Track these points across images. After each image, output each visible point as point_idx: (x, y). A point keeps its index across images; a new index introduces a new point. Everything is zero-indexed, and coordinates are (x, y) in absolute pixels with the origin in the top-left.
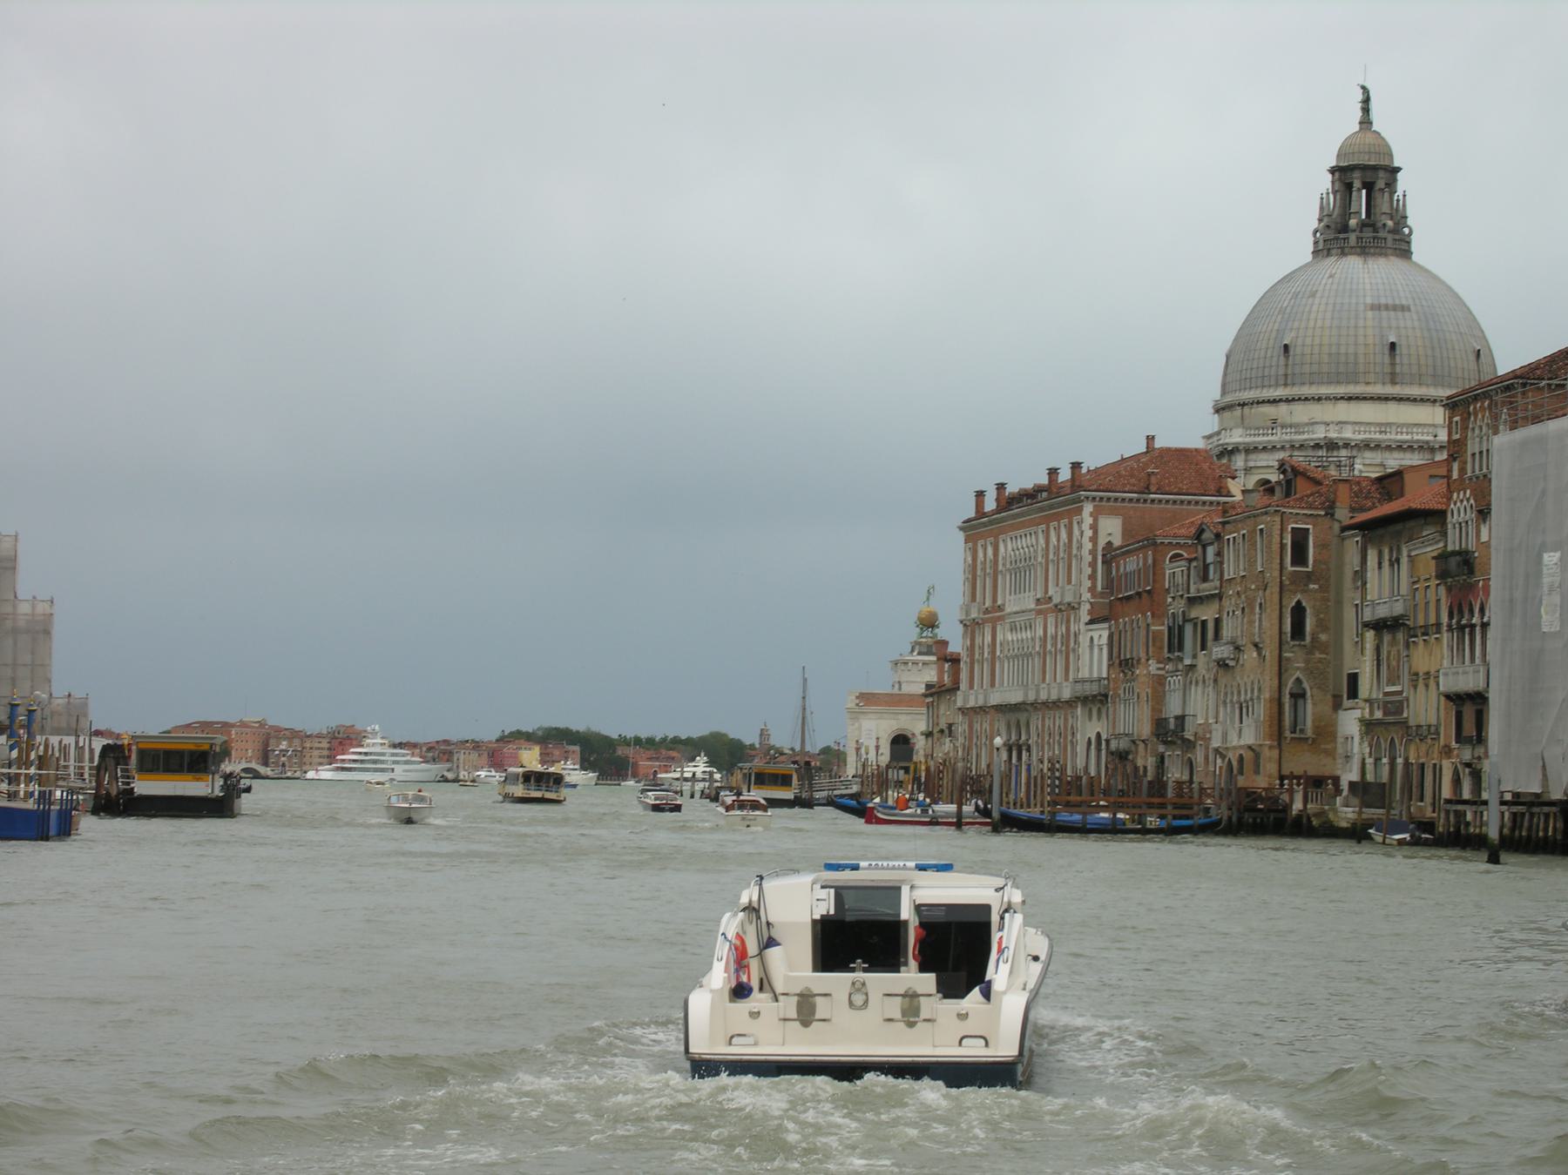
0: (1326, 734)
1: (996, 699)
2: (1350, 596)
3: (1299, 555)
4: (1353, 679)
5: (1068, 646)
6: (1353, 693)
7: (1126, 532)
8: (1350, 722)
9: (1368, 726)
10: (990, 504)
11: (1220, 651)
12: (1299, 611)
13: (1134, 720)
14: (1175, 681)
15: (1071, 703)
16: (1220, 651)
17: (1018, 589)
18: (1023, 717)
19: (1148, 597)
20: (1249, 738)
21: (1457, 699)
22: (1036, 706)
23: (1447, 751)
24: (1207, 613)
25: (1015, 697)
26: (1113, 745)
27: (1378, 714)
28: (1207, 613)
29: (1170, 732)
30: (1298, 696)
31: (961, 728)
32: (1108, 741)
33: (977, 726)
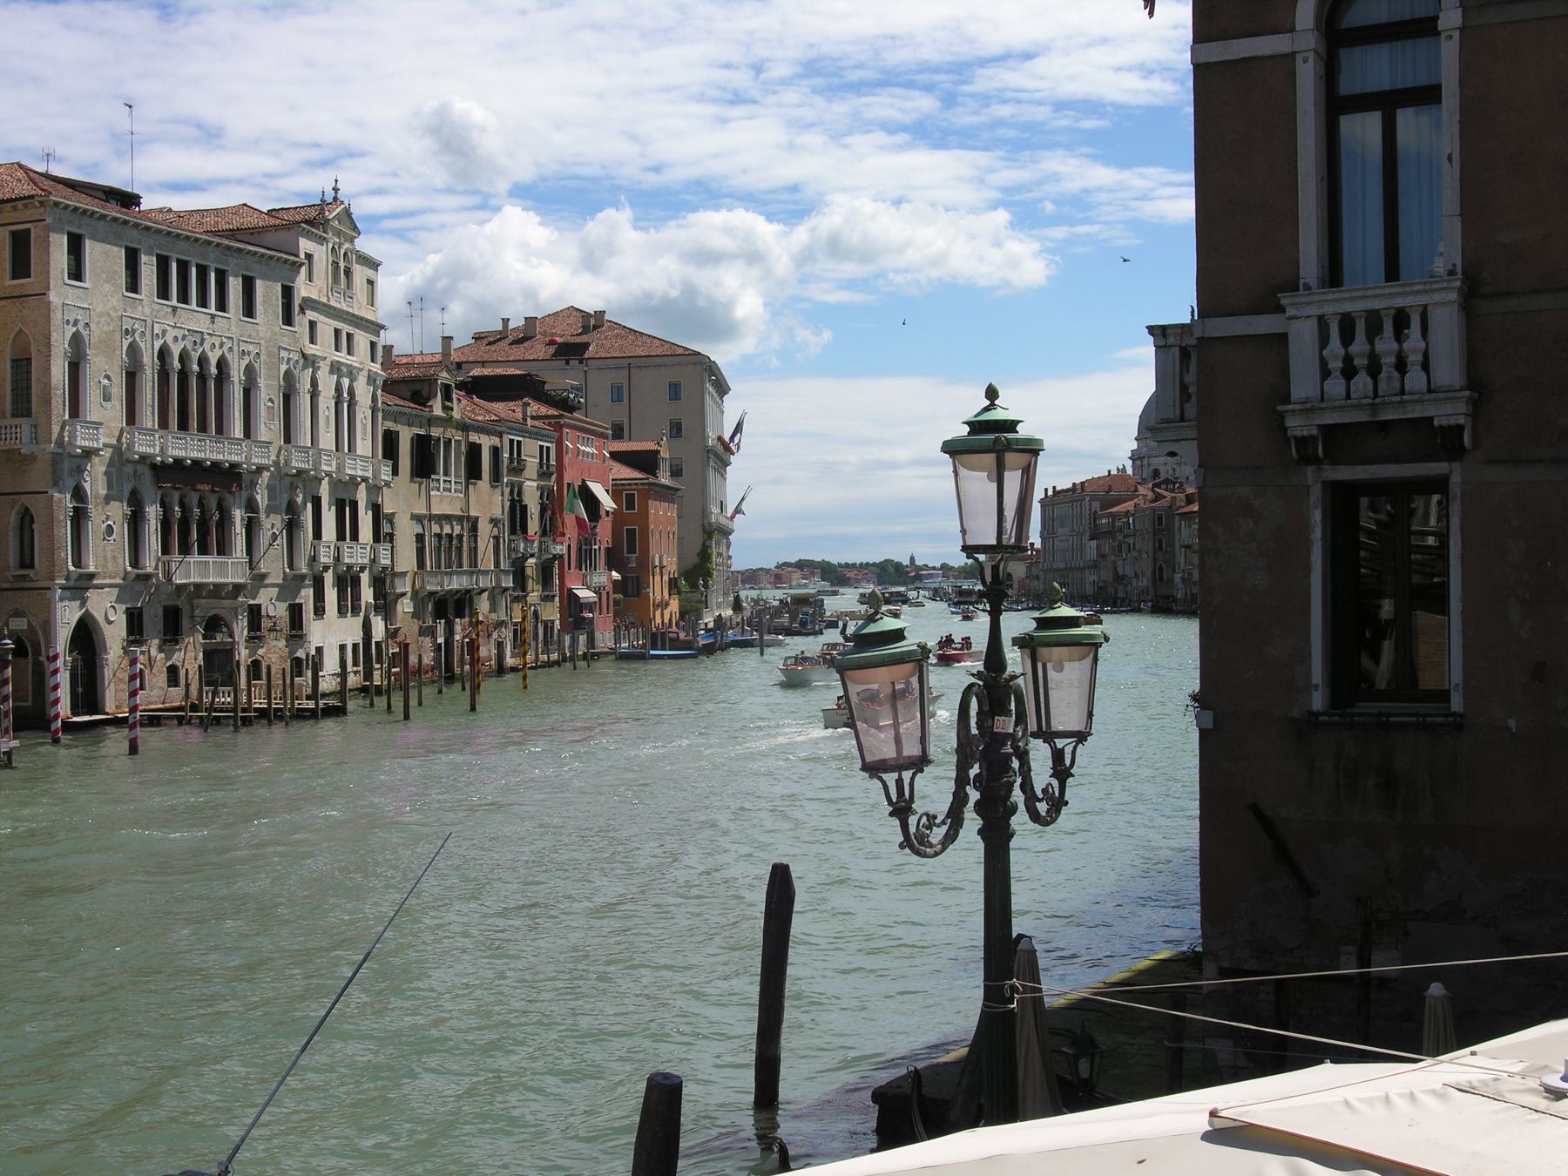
0: (1171, 581)
1: (1055, 566)
2: (1177, 537)
3: (1160, 523)
5: (1082, 548)
7: (1103, 508)
8: (1177, 578)
9: (1183, 579)
10: (1050, 493)
11: (1135, 554)
12: (1160, 542)
13: (1107, 575)
14: (1120, 563)
16: (1135, 554)
17: (1062, 525)
19: (1111, 534)
24: (1131, 541)
25: (1063, 565)
28: (1131, 541)
29: (1119, 579)
30: (1161, 569)
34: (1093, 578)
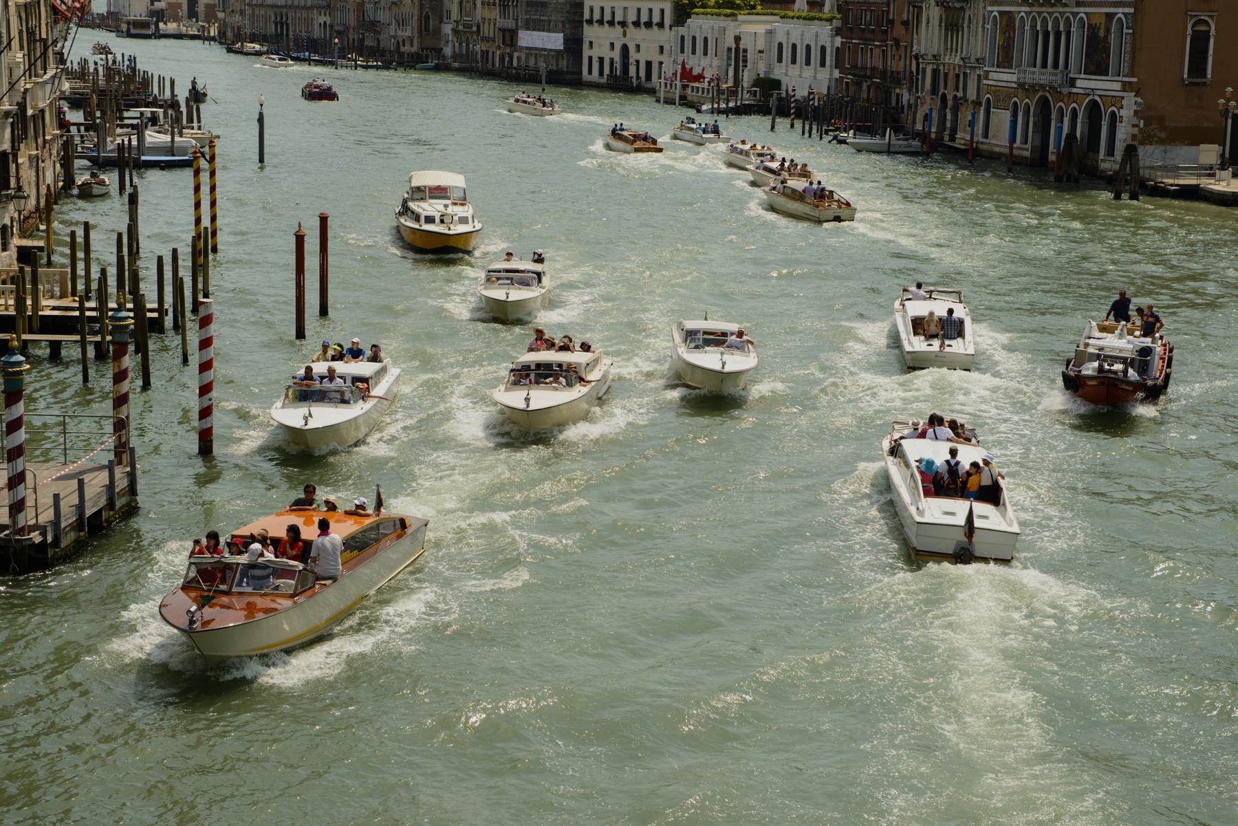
0: (437, 32)
4: (449, 12)
6: (449, 17)
8: (447, 29)
9: (455, 32)
15: (312, 8)
18: (284, 11)
20: (408, 33)
21: (503, 31)
22: (291, 7)
23: (499, 47)
26: (336, 28)
27: (461, 28)
30: (427, 17)
31: (248, 11)
32: (331, 26)
33: (257, 12)
34: (322, 19)
